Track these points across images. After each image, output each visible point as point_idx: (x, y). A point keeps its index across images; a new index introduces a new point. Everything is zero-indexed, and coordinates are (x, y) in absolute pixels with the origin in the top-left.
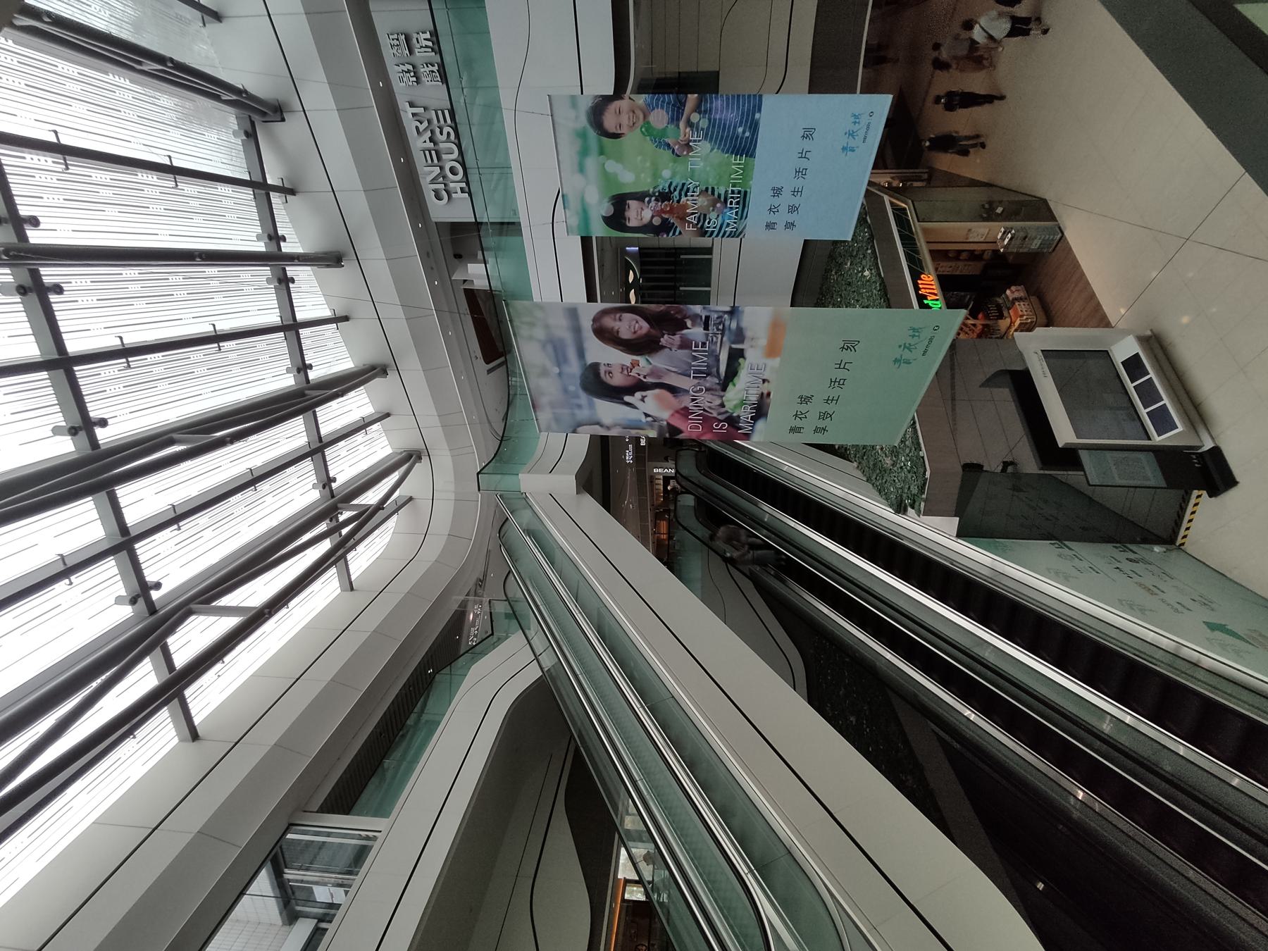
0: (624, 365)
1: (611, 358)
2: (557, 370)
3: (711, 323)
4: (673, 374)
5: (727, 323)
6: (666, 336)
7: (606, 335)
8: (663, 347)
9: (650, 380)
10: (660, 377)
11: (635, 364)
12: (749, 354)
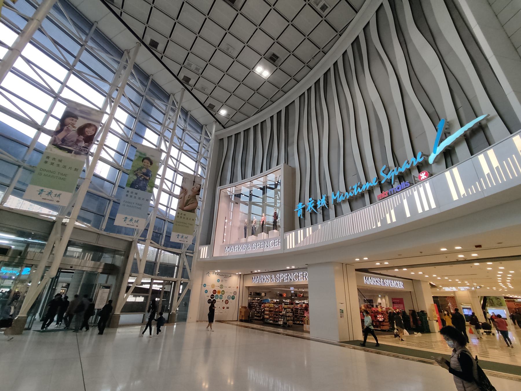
0: (75, 124)
1: (80, 123)
2: (78, 109)
3: (85, 149)
4: (66, 134)
5: (84, 152)
6: (83, 138)
7: (89, 125)
8: (79, 136)
9: (65, 128)
10: (66, 131)
11: (74, 127)
12: (69, 154)
